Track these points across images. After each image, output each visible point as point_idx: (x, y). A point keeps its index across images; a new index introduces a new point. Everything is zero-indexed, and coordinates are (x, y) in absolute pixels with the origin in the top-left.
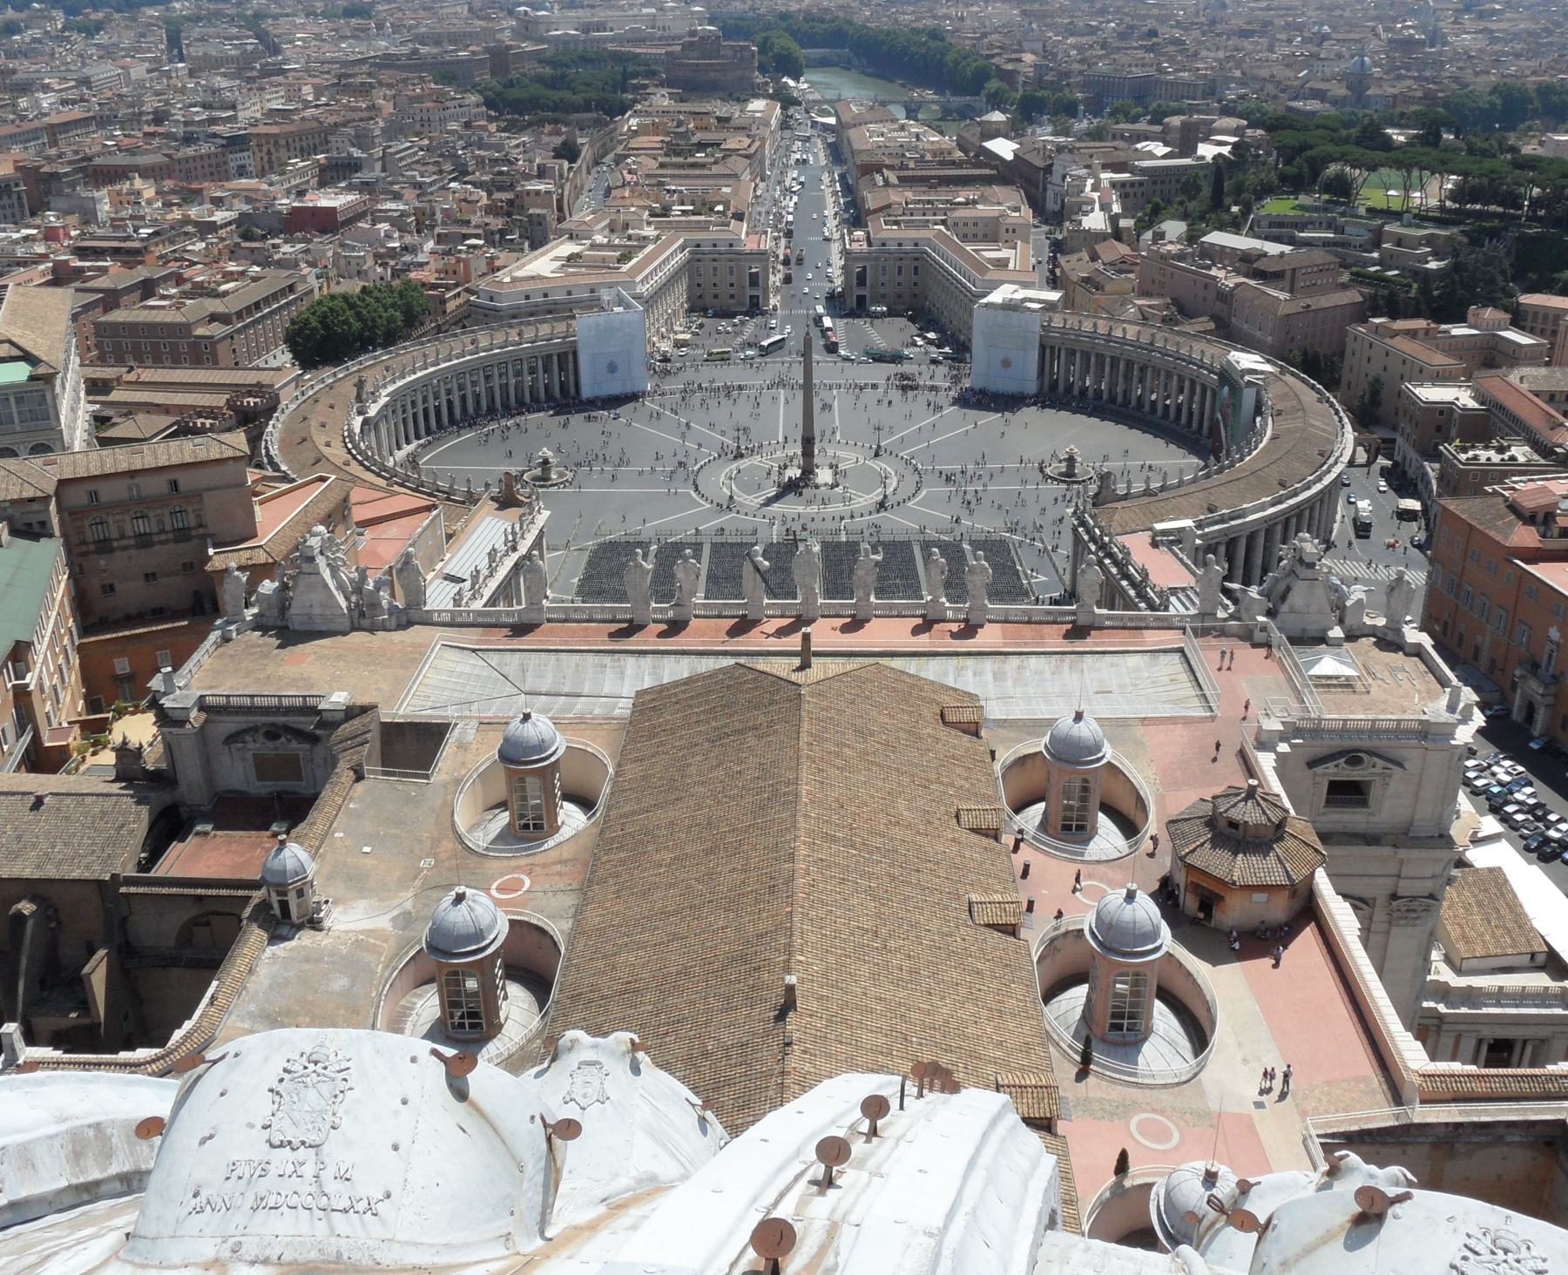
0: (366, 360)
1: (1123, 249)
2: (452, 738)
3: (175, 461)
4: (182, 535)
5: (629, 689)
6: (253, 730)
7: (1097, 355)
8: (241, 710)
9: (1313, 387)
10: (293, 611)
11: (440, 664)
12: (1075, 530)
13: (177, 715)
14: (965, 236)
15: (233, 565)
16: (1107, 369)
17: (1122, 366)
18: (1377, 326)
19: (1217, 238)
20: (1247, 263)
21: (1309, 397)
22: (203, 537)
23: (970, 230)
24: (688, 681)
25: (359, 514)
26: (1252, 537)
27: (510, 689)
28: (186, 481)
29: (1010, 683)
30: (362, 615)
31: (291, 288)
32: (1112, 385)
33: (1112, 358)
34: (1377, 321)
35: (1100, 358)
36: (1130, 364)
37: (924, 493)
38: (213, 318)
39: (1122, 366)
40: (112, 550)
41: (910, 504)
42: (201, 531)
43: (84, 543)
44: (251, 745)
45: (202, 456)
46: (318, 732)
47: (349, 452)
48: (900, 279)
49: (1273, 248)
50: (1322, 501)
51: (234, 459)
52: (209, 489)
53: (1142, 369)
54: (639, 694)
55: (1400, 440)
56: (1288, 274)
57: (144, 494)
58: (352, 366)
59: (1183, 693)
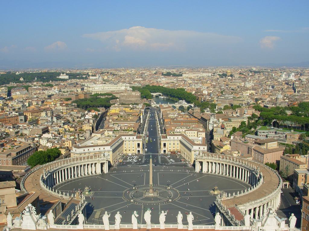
14: (190, 136)
15: (9, 213)
17: (228, 166)
19: (249, 135)
21: (272, 173)
22: (4, 206)
23: (191, 134)
26: (259, 207)
31: (30, 147)
34: (287, 154)
35: (223, 164)
37: (180, 198)
39: (228, 166)
41: (176, 201)
42: (4, 204)
48: (174, 146)
50: (276, 198)
52: (6, 195)
55: (294, 184)
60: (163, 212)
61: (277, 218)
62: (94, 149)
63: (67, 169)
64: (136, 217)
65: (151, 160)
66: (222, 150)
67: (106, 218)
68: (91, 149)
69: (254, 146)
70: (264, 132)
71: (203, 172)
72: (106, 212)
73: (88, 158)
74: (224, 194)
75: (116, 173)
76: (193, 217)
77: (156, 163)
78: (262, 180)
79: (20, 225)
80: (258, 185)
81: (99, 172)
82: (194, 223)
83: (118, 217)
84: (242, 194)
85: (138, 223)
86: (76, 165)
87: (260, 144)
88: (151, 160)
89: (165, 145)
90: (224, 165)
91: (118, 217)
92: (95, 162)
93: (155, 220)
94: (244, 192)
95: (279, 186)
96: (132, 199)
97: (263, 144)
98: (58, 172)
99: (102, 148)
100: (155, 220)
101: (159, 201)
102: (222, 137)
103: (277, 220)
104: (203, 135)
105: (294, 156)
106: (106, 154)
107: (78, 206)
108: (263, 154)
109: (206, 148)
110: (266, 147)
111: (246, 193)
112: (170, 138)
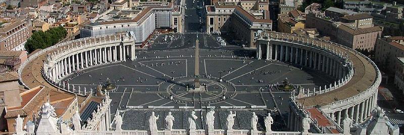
0: (49, 49)
1: (300, 12)
7: (293, 48)
9: (367, 59)
12: (290, 107)
14: (246, 8)
16: (297, 52)
17: (302, 51)
18: (387, 38)
20: (339, 17)
21: (365, 62)
23: (248, 6)
30: (61, 132)
32: (299, 58)
33: (299, 49)
34: (387, 37)
36: (304, 51)
39: (302, 51)
47: (43, 77)
49: (351, 13)
53: (308, 53)
56: (356, 21)
58: (44, 51)
60: (231, 112)
61: (389, 123)
62: (115, 27)
63: (79, 54)
64: (193, 119)
65: (197, 41)
66: (293, 29)
67: (153, 120)
68: (111, 26)
69: (338, 24)
70: (353, 5)
71: (268, 59)
72: (153, 113)
73: (108, 38)
74: (301, 91)
75: (146, 60)
76: (273, 121)
77: (201, 46)
78: (352, 71)
80: (347, 78)
81: (123, 58)
82: (274, 128)
83: (170, 119)
84: (327, 90)
85: (197, 129)
86: (91, 49)
87: (347, 21)
88: (197, 41)
89: (212, 19)
90: (297, 50)
91: (170, 119)
92: (119, 44)
93: (220, 123)
94: (328, 87)
95: (376, 80)
96: (171, 96)
97: (354, 21)
98: (67, 58)
99: (126, 25)
100: (220, 123)
101: (208, 99)
102: (292, 10)
103: (388, 126)
104: (266, 7)
105: (397, 39)
106: (132, 33)
107: (101, 105)
108: (353, 35)
109: (271, 27)
110: (356, 26)
111: (331, 89)
112: (219, 11)
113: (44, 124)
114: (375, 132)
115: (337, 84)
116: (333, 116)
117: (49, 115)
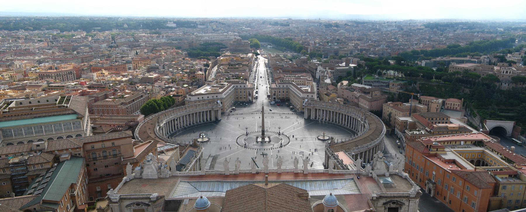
2: (184, 203)
3: (114, 138)
4: (115, 156)
5: (225, 190)
6: (134, 203)
8: (130, 199)
10: (144, 173)
11: (180, 185)
13: (114, 201)
22: (121, 156)
24: (239, 188)
25: (159, 150)
27: (196, 191)
28: (117, 143)
29: (313, 187)
38: (122, 104)
40: (97, 160)
43: (90, 158)
44: (133, 207)
45: (121, 136)
46: (150, 203)
51: (129, 137)
54: (227, 191)
57: (106, 146)
59: (353, 189)
79: (141, 174)
98: (171, 121)
113: (148, 168)
114: (377, 169)
115: (357, 135)
116: (354, 157)
117: (151, 162)
